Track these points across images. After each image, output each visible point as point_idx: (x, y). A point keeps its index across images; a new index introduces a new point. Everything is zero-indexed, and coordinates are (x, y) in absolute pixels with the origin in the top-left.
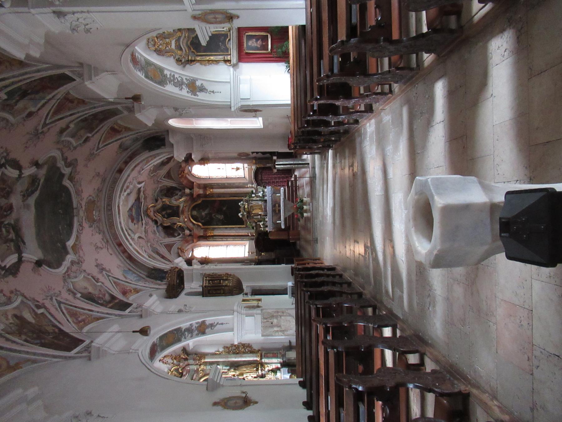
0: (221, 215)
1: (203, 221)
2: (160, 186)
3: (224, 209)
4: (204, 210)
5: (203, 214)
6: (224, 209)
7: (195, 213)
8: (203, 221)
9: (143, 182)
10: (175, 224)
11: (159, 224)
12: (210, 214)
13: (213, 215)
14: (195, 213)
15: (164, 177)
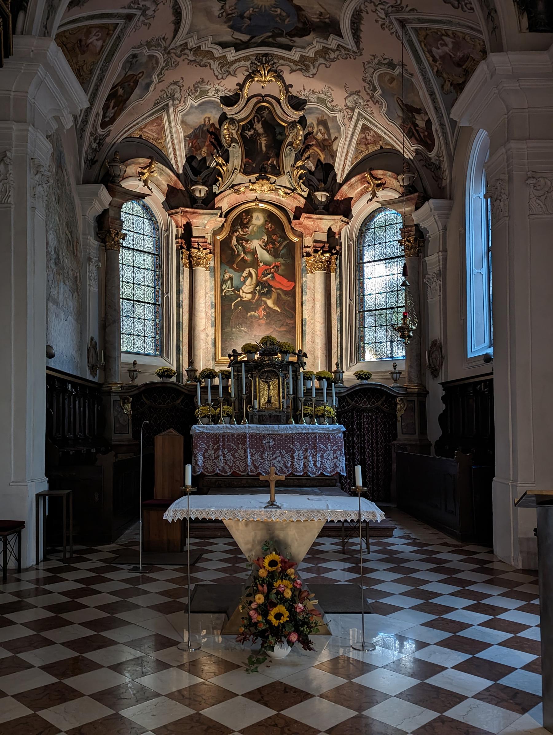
0: (253, 293)
1: (234, 242)
2: (339, 116)
3: (270, 303)
4: (265, 247)
5: (256, 244)
6: (270, 303)
7: (258, 220)
8: (234, 242)
9: (358, 48)
10: (227, 161)
11: (226, 109)
12: (255, 263)
13: (252, 271)
14: (258, 220)
15: (365, 128)
